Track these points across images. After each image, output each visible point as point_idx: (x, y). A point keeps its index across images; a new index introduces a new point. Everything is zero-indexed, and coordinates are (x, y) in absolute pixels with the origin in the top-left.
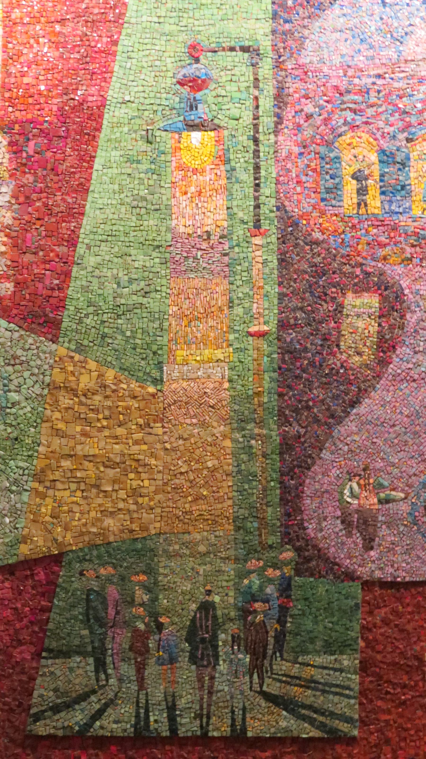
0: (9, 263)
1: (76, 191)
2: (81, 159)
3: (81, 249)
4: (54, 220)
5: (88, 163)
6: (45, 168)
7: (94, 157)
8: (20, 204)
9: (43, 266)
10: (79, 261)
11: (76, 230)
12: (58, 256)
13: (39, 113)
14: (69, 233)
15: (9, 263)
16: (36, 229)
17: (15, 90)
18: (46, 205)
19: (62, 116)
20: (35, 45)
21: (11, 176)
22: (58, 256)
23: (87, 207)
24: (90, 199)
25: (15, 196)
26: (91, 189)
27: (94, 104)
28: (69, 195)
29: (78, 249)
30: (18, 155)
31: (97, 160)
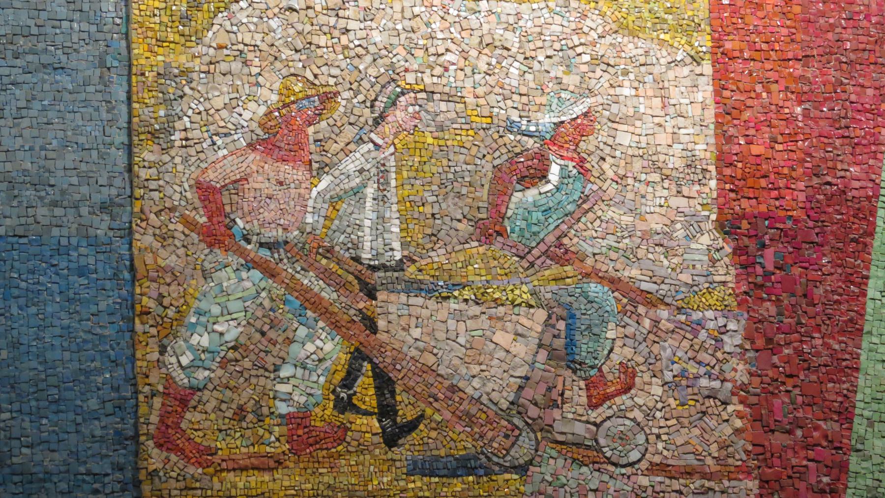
0: (750, 448)
1: (842, 332)
2: (848, 280)
3: (859, 427)
4: (814, 377)
5: (858, 285)
6: (793, 294)
7: (867, 278)
8: (757, 351)
9: (803, 453)
10: (859, 446)
11: (850, 395)
12: (826, 437)
13: (777, 203)
14: (840, 399)
15: (750, 448)
16: (787, 391)
17: (740, 165)
18: (799, 353)
19: (813, 210)
20: (764, 95)
21: (739, 304)
22: (826, 437)
23: (863, 358)
24: (865, 344)
25: (748, 337)
26: (867, 328)
27: (862, 193)
28: (834, 338)
29: (855, 426)
30: (750, 270)
31: (871, 282)
